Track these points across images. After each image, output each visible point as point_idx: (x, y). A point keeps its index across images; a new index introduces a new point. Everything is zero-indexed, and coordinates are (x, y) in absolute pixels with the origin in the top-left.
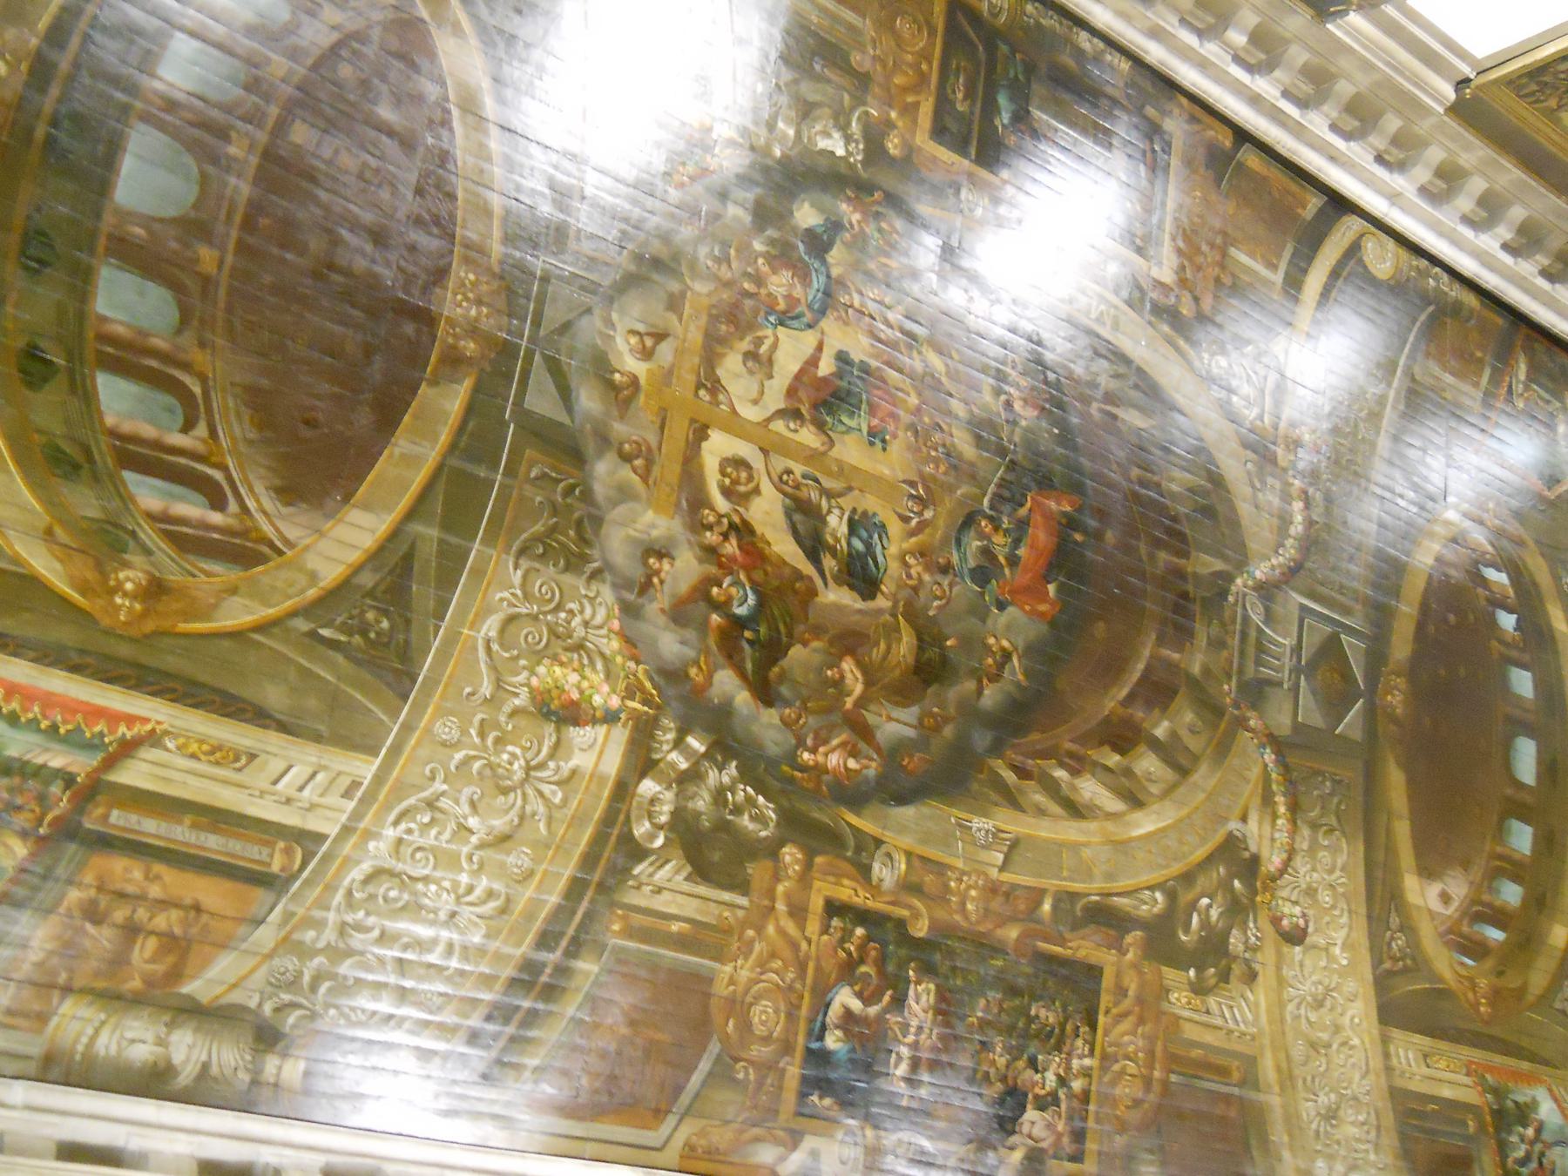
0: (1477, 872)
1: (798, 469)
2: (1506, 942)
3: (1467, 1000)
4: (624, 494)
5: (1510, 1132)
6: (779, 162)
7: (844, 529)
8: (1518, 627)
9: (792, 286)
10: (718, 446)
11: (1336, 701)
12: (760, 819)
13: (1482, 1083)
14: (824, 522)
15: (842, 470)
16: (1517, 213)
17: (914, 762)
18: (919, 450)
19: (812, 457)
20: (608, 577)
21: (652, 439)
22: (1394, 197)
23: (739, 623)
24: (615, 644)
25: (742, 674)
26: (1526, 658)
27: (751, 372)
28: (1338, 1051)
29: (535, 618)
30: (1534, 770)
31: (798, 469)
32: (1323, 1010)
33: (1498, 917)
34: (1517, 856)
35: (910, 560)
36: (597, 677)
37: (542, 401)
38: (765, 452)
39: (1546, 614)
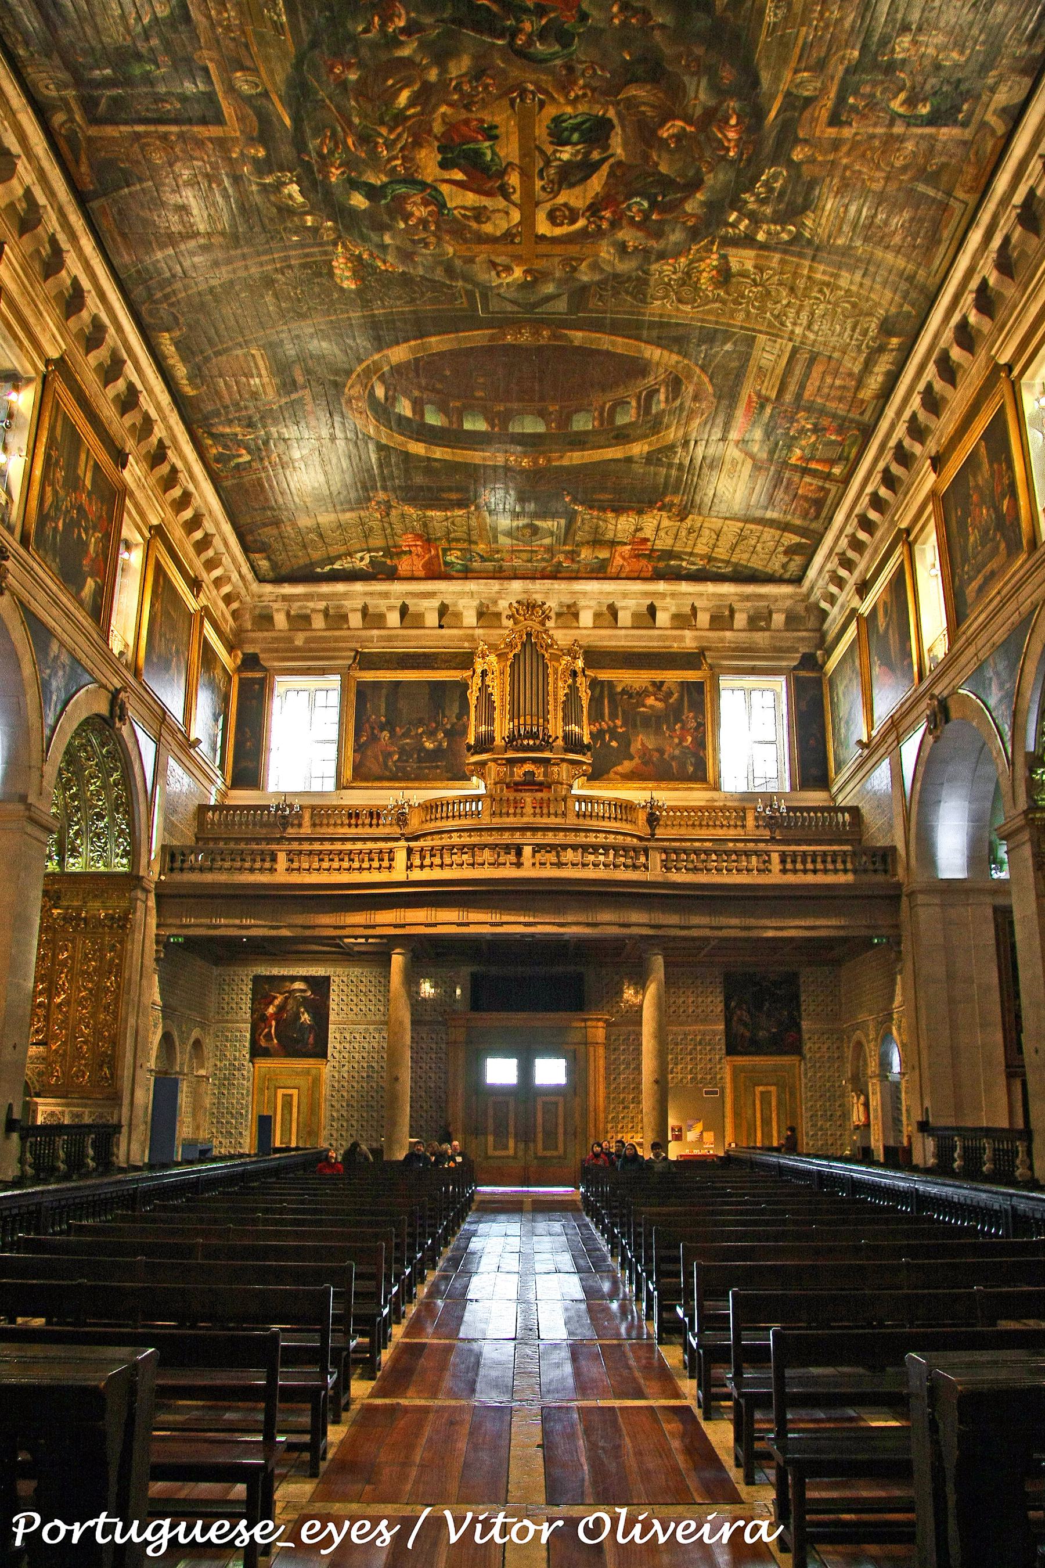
1: (539, 184)
4: (595, 266)
6: (335, 221)
7: (568, 148)
9: (415, 203)
10: (543, 227)
12: (775, 177)
14: (569, 162)
15: (525, 153)
17: (728, 75)
18: (483, 99)
19: (526, 176)
20: (645, 267)
21: (557, 260)
23: (654, 205)
24: (682, 260)
25: (683, 200)
27: (489, 219)
29: (676, 293)
31: (539, 184)
35: (572, 95)
36: (703, 265)
37: (561, 306)
38: (537, 204)
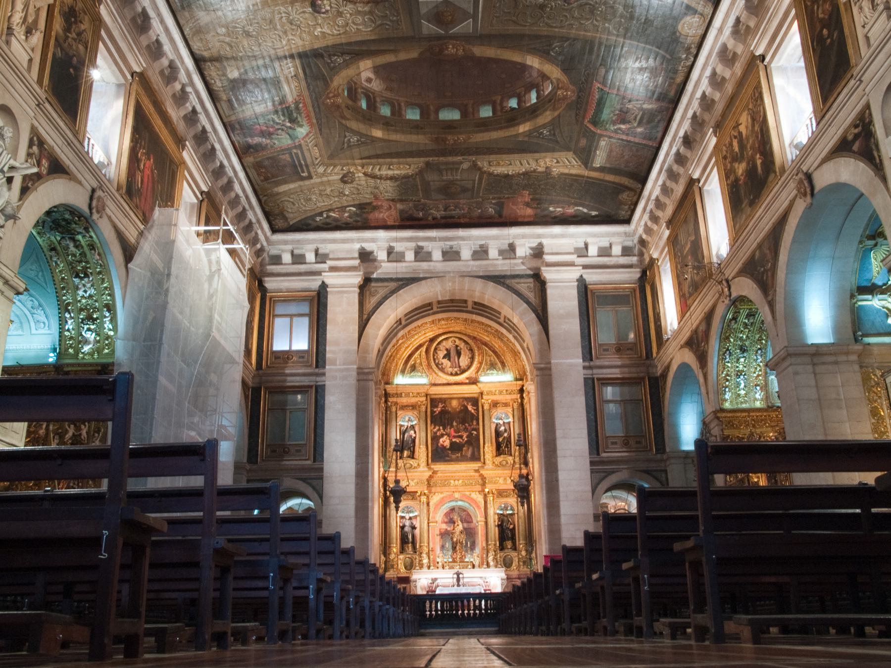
0: (388, 94)
2: (363, 110)
3: (328, 93)
5: (284, 115)
8: (513, 109)
11: (438, 17)
13: (297, 103)
16: (717, 96)
22: (721, 30)
26: (499, 113)
28: (275, 34)
30: (446, 118)
32: (289, 24)
33: (372, 105)
34: (403, 112)
39: (524, 122)
